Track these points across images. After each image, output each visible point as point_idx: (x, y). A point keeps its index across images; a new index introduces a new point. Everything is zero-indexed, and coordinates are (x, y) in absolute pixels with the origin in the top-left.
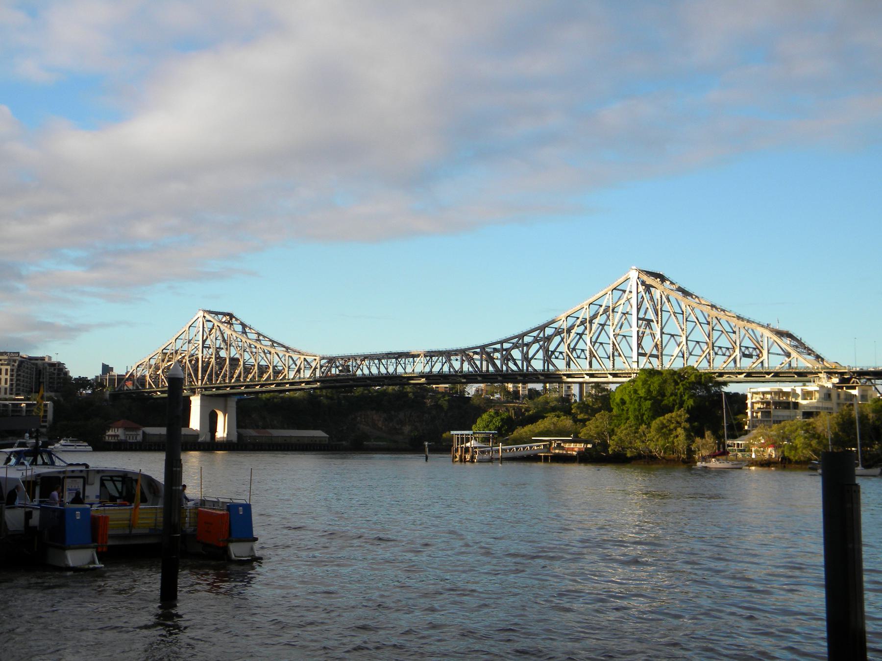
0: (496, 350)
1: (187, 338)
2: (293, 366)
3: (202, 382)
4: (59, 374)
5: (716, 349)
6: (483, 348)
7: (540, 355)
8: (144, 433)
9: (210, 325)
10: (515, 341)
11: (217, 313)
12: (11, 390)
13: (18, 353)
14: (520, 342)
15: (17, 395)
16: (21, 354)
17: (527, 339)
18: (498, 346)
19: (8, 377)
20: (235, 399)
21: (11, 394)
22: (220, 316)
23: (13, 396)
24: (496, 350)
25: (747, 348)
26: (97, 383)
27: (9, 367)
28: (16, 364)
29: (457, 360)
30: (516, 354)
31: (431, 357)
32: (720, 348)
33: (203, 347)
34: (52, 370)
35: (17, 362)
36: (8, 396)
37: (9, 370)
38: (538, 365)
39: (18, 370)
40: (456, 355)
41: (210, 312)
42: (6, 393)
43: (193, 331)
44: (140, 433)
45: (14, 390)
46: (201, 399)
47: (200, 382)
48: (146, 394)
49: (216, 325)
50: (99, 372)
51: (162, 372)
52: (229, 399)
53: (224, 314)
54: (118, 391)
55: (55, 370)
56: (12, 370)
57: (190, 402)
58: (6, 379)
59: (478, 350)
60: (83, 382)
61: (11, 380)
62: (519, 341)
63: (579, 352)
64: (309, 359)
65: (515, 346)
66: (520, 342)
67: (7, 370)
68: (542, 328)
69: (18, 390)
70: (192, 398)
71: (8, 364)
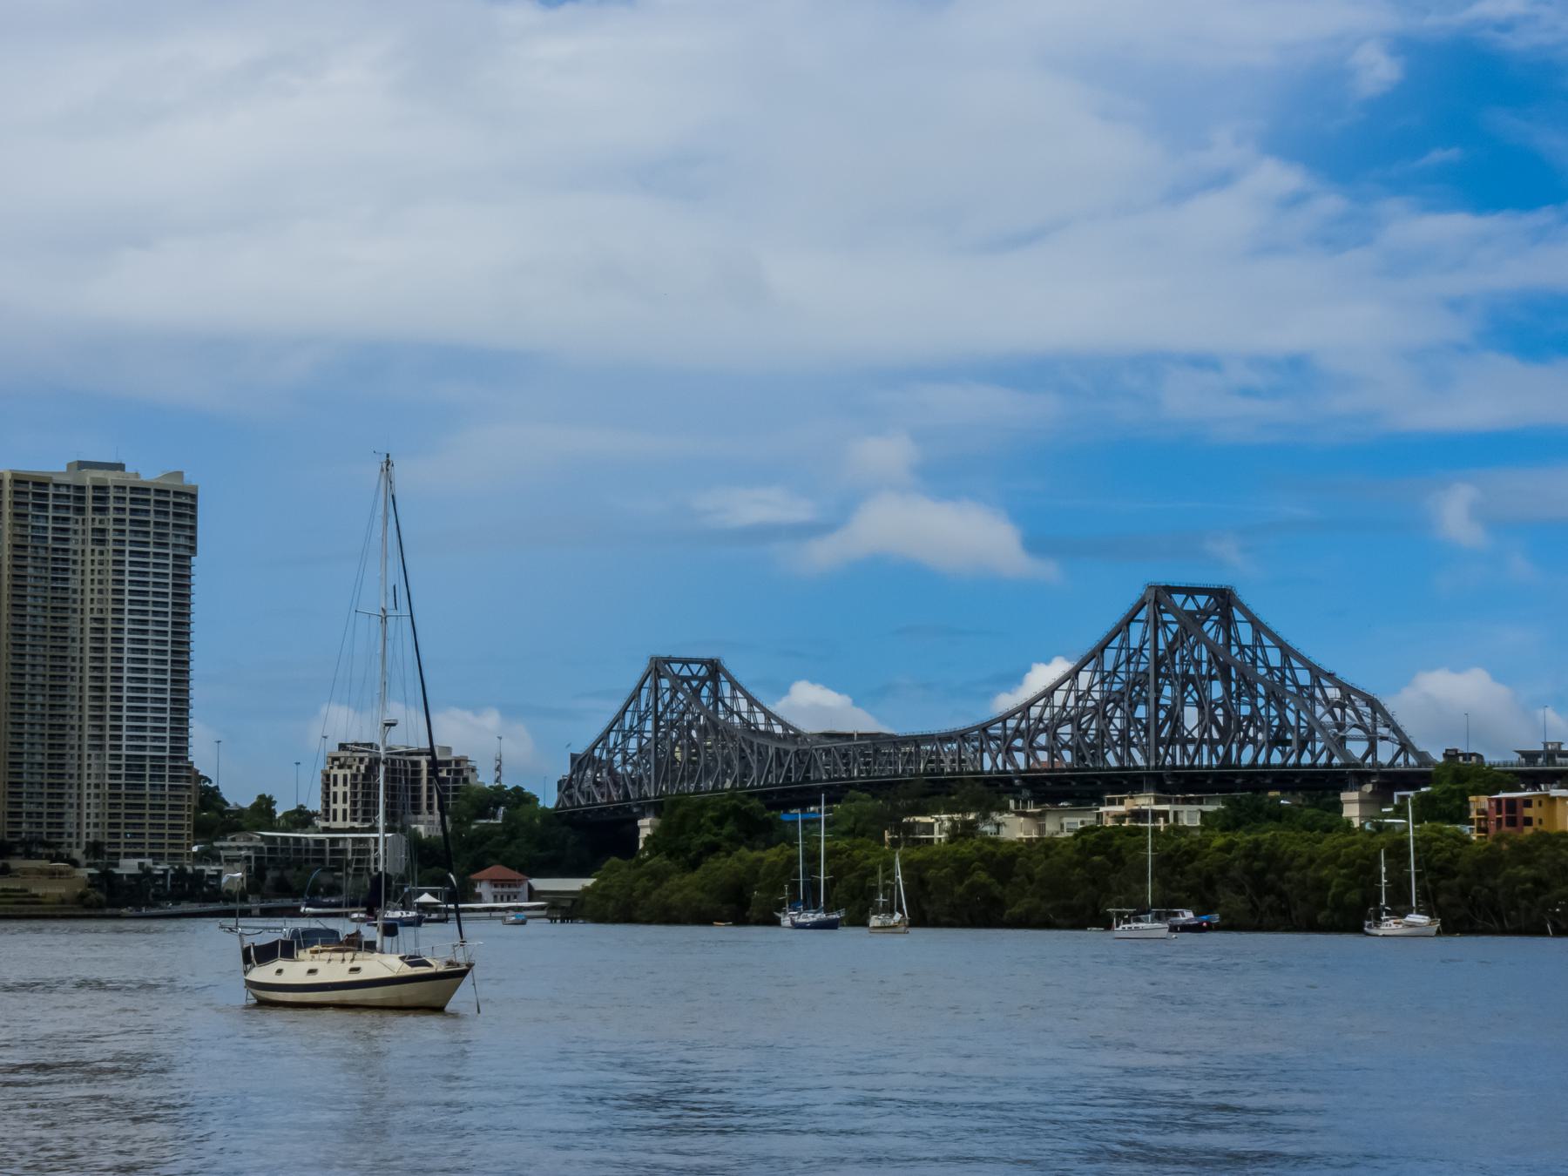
3: (655, 794)
4: (456, 781)
8: (530, 887)
11: (686, 662)
12: (354, 812)
15: (364, 821)
19: (348, 789)
22: (695, 668)
23: (356, 825)
27: (348, 772)
28: (362, 768)
35: (367, 760)
36: (349, 824)
39: (364, 776)
41: (669, 661)
42: (345, 819)
44: (526, 886)
45: (360, 813)
47: (653, 794)
53: (702, 662)
55: (449, 772)
56: (354, 777)
58: (345, 794)
61: (354, 795)
67: (345, 777)
70: (640, 823)
71: (350, 767)
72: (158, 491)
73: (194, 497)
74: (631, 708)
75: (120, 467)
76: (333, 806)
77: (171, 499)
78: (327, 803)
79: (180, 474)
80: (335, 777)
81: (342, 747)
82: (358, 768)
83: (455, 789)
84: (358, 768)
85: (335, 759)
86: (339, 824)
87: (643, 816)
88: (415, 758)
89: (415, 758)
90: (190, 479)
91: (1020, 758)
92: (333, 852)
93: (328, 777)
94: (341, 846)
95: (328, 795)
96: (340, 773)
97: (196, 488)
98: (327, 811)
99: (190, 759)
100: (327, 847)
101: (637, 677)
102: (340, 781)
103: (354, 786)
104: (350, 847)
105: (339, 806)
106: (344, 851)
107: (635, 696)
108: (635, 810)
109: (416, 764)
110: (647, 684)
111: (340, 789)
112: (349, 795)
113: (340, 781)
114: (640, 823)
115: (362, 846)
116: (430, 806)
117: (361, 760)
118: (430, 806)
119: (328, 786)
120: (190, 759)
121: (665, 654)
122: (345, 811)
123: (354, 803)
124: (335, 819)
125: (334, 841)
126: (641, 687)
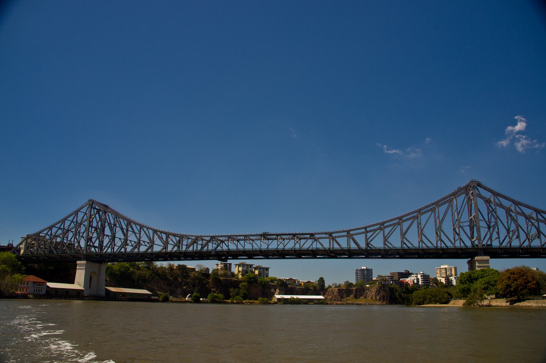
1: (75, 220)
43: (81, 215)
52: (102, 265)
57: (76, 265)
74: (71, 218)
110: (84, 210)
114: (78, 262)
126: (78, 211)
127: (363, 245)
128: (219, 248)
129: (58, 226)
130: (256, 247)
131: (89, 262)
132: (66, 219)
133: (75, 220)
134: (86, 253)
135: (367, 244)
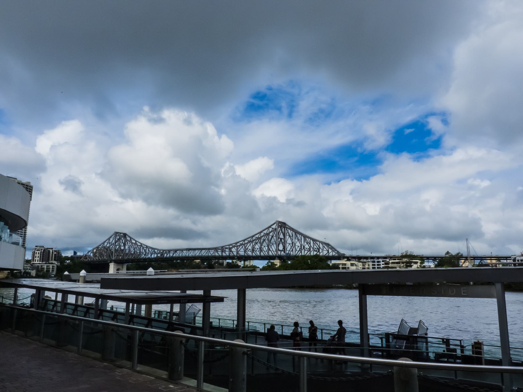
0: (226, 248)
1: (109, 242)
2: (150, 253)
5: (305, 249)
6: (222, 247)
7: (242, 250)
9: (118, 237)
10: (234, 245)
11: (121, 233)
12: (40, 260)
13: (43, 246)
14: (236, 245)
15: (42, 262)
16: (44, 247)
17: (238, 244)
18: (228, 247)
19: (39, 255)
20: (126, 264)
21: (40, 262)
22: (122, 234)
23: (41, 263)
24: (226, 248)
25: (315, 248)
26: (71, 259)
27: (40, 252)
28: (42, 251)
29: (212, 251)
30: (234, 250)
31: (202, 250)
32: (306, 248)
33: (115, 245)
34: (56, 253)
35: (43, 249)
36: (39, 262)
37: (40, 253)
38: (242, 253)
40: (212, 250)
42: (38, 261)
43: (111, 239)
45: (41, 260)
46: (114, 265)
47: (113, 258)
48: (92, 263)
49: (121, 237)
50: (73, 254)
51: (99, 254)
54: (121, 259)
55: (57, 253)
56: (41, 253)
57: (109, 265)
58: (38, 256)
59: (220, 248)
60: (67, 258)
61: (40, 256)
62: (236, 245)
63: (248, 250)
64: (156, 251)
65: (234, 247)
66: (236, 245)
68: (244, 240)
69: (42, 260)
70: (110, 264)
71: (39, 251)
72: (27, 185)
73: (32, 188)
74: (107, 241)
75: (16, 179)
76: (35, 259)
77: (29, 187)
78: (34, 258)
79: (30, 183)
80: (36, 253)
81: (36, 246)
82: (41, 251)
83: (58, 256)
84: (41, 251)
85: (35, 249)
86: (36, 262)
87: (111, 262)
88: (49, 250)
89: (49, 250)
90: (32, 184)
91: (220, 253)
92: (41, 268)
93: (34, 252)
94: (43, 267)
95: (34, 256)
96: (38, 252)
97: (33, 186)
98: (33, 260)
99: (25, 246)
100: (40, 267)
101: (110, 236)
102: (37, 253)
103: (41, 255)
104: (45, 267)
105: (37, 259)
106: (44, 268)
107: (109, 239)
108: (109, 261)
109: (49, 251)
110: (113, 237)
111: (37, 255)
112: (39, 256)
113: (37, 253)
114: (110, 264)
115: (49, 267)
116: (52, 260)
117: (42, 249)
118: (52, 260)
119: (34, 254)
120: (25, 246)
121: (117, 231)
122: (38, 260)
123: (40, 258)
124: (35, 261)
125: (42, 266)
126: (110, 237)
127: (235, 254)
128: (168, 256)
129: (102, 245)
130: (184, 255)
131: (115, 264)
132: (105, 242)
133: (109, 242)
134: (114, 259)
135: (237, 253)
